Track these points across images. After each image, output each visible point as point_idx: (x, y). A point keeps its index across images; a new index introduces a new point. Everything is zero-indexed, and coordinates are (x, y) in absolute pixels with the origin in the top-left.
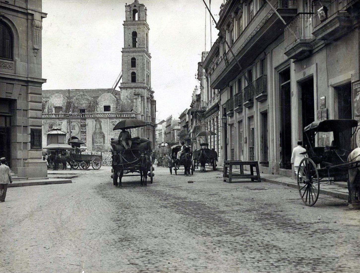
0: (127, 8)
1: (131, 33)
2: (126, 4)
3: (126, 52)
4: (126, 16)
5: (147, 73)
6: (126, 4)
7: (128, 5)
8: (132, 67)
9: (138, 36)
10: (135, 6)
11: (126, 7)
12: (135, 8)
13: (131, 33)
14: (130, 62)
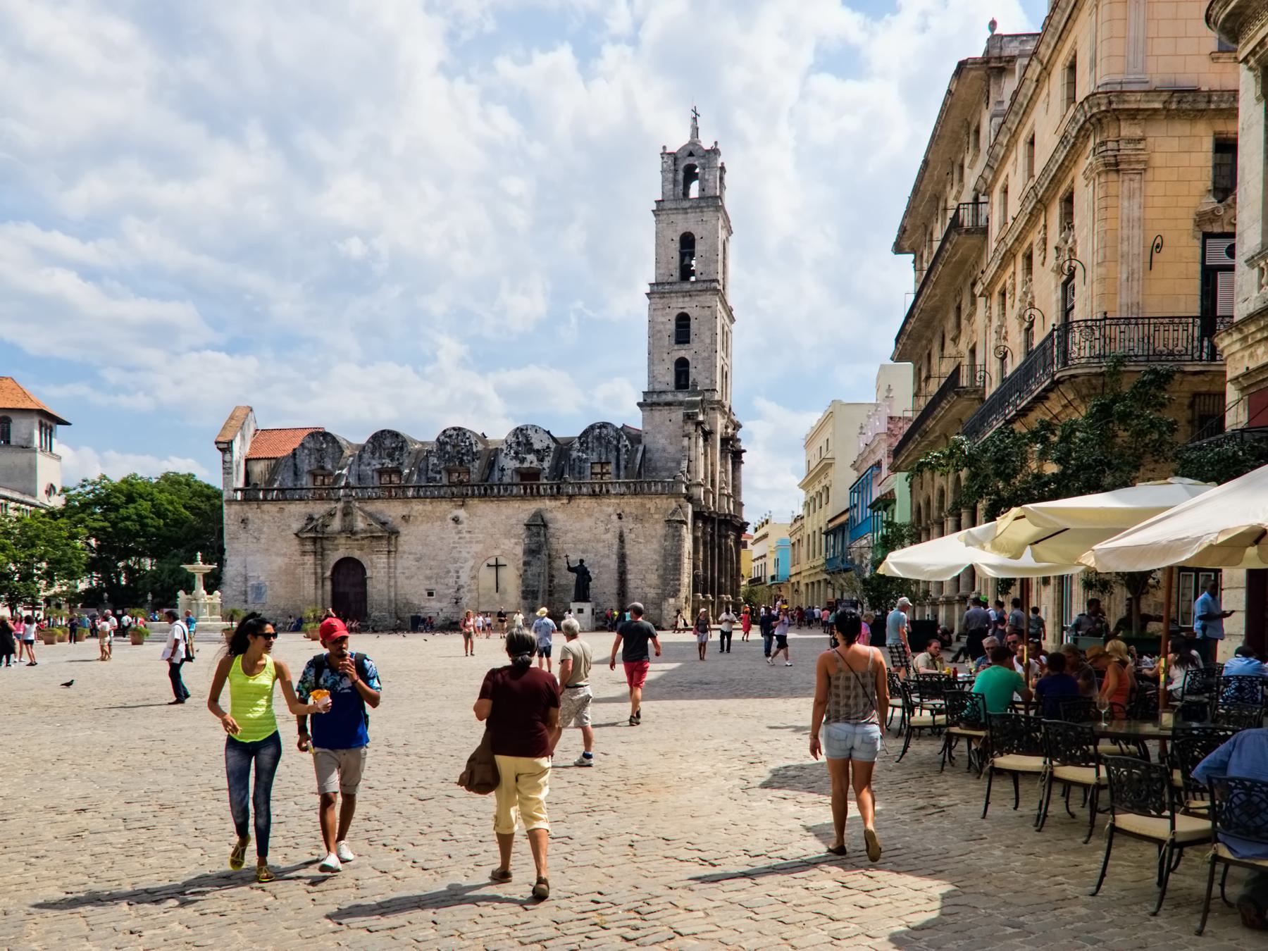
1: (677, 239)
3: (662, 295)
4: (663, 187)
5: (722, 363)
8: (678, 342)
9: (699, 248)
14: (672, 326)
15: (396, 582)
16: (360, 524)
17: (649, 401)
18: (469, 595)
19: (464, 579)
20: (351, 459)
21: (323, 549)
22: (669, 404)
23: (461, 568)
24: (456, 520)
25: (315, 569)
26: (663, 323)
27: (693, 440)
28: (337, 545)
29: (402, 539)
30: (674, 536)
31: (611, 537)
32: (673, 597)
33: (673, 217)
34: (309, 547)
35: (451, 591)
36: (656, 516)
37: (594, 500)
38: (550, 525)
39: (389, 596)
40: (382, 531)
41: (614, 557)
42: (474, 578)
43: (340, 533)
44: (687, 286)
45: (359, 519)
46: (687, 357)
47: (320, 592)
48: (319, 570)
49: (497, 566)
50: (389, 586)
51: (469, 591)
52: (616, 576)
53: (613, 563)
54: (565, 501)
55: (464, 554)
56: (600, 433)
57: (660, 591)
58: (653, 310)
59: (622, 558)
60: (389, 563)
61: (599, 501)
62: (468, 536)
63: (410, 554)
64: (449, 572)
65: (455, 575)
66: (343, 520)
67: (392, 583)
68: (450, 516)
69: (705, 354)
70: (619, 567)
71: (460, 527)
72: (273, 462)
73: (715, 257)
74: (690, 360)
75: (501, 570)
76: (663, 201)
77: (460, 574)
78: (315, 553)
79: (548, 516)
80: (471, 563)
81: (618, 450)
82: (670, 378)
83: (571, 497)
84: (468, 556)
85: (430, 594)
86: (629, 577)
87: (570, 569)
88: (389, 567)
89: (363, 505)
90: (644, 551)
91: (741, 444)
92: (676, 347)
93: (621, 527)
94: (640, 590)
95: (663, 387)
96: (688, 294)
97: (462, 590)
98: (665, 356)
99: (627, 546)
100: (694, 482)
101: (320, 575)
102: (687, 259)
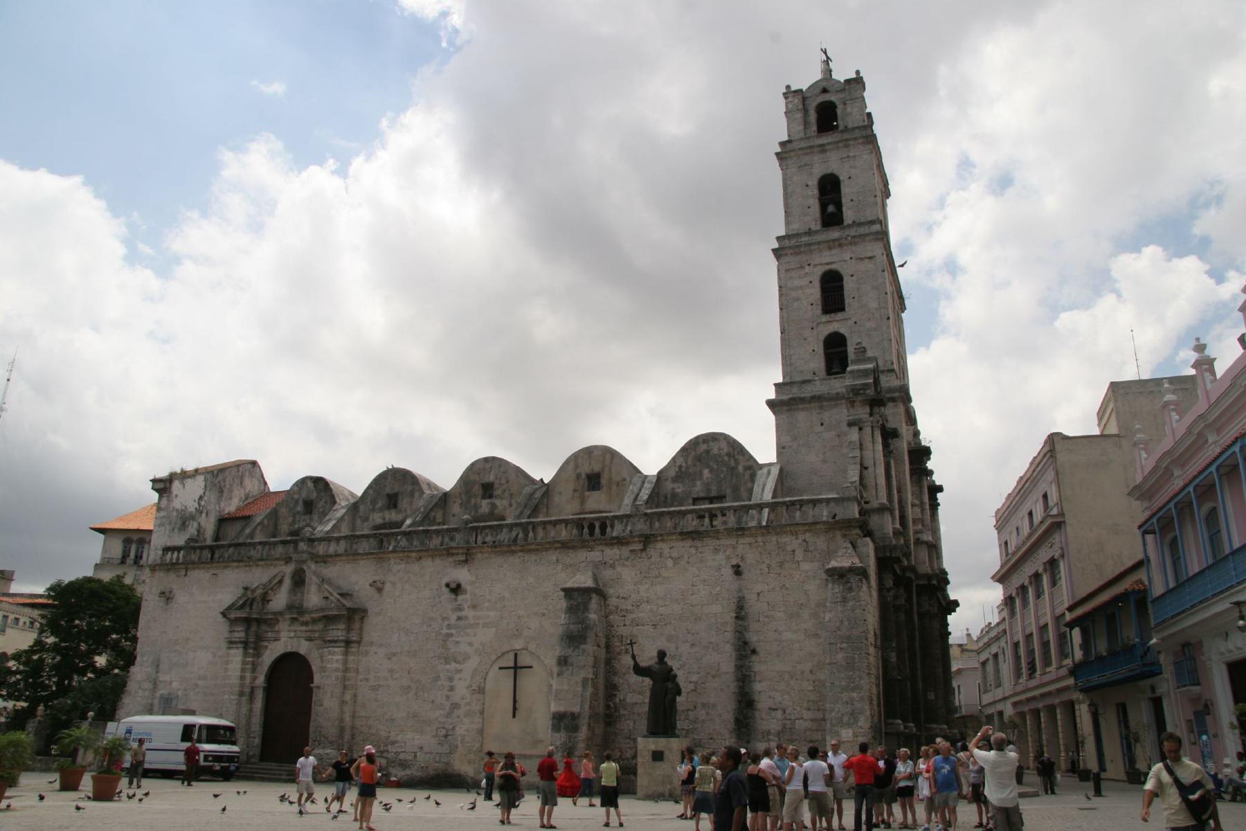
0: (790, 99)
1: (814, 182)
2: (788, 87)
3: (797, 251)
7: (793, 88)
10: (825, 91)
11: (786, 98)
12: (826, 97)
13: (816, 183)
14: (815, 292)
16: (313, 598)
17: (785, 397)
19: (461, 689)
21: (260, 638)
22: (817, 399)
23: (459, 671)
24: (456, 589)
25: (243, 670)
26: (801, 288)
27: (868, 430)
28: (278, 632)
29: (372, 620)
31: (722, 611)
32: (849, 725)
33: (806, 159)
34: (240, 634)
35: (438, 713)
36: (806, 566)
39: (342, 720)
41: (729, 648)
44: (835, 234)
45: (313, 588)
46: (842, 331)
47: (244, 710)
48: (248, 675)
49: (516, 668)
50: (343, 703)
51: (467, 715)
52: (733, 686)
53: (725, 661)
54: (639, 546)
55: (464, 648)
56: (708, 452)
58: (783, 274)
59: (745, 651)
60: (345, 662)
61: (698, 543)
63: (381, 645)
64: (438, 678)
65: (447, 684)
67: (348, 697)
71: (460, 598)
73: (872, 199)
74: (846, 335)
76: (789, 141)
77: (455, 682)
78: (245, 644)
80: (473, 663)
82: (818, 363)
83: (647, 540)
84: (469, 650)
86: (757, 686)
87: (639, 670)
88: (346, 670)
90: (788, 635)
91: (934, 477)
92: (825, 318)
93: (740, 590)
94: (779, 714)
96: (839, 244)
97: (457, 712)
98: (807, 333)
99: (754, 626)
101: (248, 681)
102: (831, 208)
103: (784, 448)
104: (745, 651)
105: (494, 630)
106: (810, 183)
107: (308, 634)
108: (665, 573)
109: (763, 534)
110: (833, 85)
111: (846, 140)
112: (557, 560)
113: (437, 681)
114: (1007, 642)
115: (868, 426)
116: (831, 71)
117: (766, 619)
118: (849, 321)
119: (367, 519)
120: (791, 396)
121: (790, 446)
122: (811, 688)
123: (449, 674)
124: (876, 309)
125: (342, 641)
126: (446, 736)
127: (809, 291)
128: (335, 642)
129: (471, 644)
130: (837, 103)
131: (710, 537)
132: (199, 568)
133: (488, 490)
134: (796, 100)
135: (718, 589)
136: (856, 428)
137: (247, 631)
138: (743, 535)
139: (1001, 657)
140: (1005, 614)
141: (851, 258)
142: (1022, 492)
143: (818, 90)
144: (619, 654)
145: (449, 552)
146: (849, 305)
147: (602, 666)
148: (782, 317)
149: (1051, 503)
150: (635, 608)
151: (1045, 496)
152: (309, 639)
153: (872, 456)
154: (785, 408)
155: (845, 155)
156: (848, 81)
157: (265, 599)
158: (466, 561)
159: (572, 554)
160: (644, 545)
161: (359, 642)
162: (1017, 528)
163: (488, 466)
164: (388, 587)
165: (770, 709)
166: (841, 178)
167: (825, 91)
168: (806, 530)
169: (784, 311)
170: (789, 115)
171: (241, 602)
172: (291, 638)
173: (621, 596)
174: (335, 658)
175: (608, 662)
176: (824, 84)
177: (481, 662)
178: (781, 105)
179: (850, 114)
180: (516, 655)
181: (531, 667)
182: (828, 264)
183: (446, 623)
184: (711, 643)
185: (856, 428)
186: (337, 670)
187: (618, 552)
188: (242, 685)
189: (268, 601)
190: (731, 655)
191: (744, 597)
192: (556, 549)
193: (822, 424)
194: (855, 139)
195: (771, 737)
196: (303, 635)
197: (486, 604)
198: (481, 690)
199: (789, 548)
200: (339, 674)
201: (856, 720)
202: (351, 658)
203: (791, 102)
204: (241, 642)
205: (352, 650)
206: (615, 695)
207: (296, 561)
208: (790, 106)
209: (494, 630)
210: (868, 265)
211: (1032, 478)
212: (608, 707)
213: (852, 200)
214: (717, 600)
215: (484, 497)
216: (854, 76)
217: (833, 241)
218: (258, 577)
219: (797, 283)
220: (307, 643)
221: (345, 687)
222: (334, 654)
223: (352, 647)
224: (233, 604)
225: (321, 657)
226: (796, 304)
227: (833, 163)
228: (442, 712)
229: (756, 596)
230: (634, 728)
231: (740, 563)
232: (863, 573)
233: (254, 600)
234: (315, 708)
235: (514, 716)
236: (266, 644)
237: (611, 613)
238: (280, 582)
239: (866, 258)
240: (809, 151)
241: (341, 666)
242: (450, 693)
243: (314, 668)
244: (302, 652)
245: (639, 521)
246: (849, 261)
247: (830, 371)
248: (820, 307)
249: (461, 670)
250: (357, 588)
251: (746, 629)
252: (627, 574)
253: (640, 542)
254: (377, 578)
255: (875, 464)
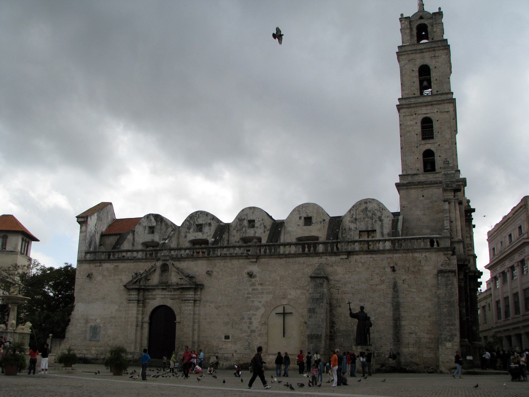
0: (403, 22)
1: (416, 69)
2: (402, 15)
3: (409, 106)
6: (402, 15)
7: (404, 16)
8: (423, 139)
10: (421, 18)
11: (401, 21)
13: (417, 69)
15: (199, 326)
16: (174, 278)
17: (405, 182)
18: (259, 338)
19: (256, 324)
20: (172, 233)
24: (251, 275)
25: (137, 314)
26: (411, 125)
27: (453, 204)
30: (447, 285)
32: (450, 341)
33: (413, 56)
35: (244, 335)
37: (369, 256)
38: (331, 278)
40: (190, 284)
41: (389, 305)
42: (265, 324)
43: (157, 286)
46: (432, 149)
47: (139, 333)
48: (140, 316)
49: (284, 314)
50: (193, 330)
51: (260, 335)
52: (391, 323)
55: (256, 304)
56: (366, 208)
57: (433, 336)
59: (397, 307)
60: (194, 310)
61: (374, 256)
62: (260, 287)
63: (212, 302)
64: (243, 318)
65: (248, 321)
66: (161, 276)
67: (196, 327)
68: (246, 271)
69: (447, 146)
70: (394, 314)
71: (253, 280)
72: (118, 237)
75: (288, 319)
77: (253, 320)
79: (329, 269)
80: (262, 311)
81: (381, 220)
82: (420, 165)
83: (349, 253)
84: (260, 305)
85: (227, 337)
86: (403, 323)
87: (352, 315)
88: (194, 314)
89: (177, 264)
92: (423, 142)
93: (395, 279)
94: (413, 335)
95: (415, 172)
100: (456, 239)
101: (140, 319)
103: (404, 207)
104: (397, 307)
105: (272, 295)
106: (414, 69)
107: (172, 296)
108: (357, 269)
109: (406, 253)
110: (426, 15)
111: (434, 47)
112: (304, 262)
113: (243, 320)
114: (491, 301)
115: (452, 202)
116: (423, 5)
117: (407, 292)
118: (436, 144)
119: (186, 237)
120: (407, 182)
121: (407, 207)
122: (429, 324)
123: (249, 316)
124: (450, 139)
125: (192, 300)
126: (249, 345)
127: (415, 128)
128: (189, 300)
129: (260, 302)
130: (428, 25)
131: (380, 253)
132: (107, 263)
133: (252, 223)
134: (407, 23)
135: (384, 277)
136: (447, 203)
137: (138, 295)
138: (396, 253)
139: (487, 308)
140: (492, 285)
141: (437, 112)
142: (506, 224)
143: (418, 17)
144: (336, 307)
145: (247, 257)
146: (436, 136)
147: (328, 313)
148: (401, 141)
149: (523, 232)
150: (343, 286)
151: (520, 228)
152: (173, 299)
153: (455, 216)
154: (405, 187)
155: (433, 56)
156: (434, 14)
157: (147, 279)
158: (256, 262)
159: (311, 259)
160: (347, 256)
161: (200, 301)
162: (501, 242)
163: (252, 211)
164: (215, 273)
165: (410, 333)
166: (431, 67)
167: (421, 18)
168: (427, 252)
169: (403, 137)
170: (403, 31)
171: (135, 280)
172: (162, 298)
173: (336, 280)
174: (189, 308)
175: (331, 311)
176: (421, 14)
177: (266, 310)
178: (398, 26)
179: (435, 32)
180: (284, 307)
181: (292, 313)
182: (425, 114)
183: (247, 292)
184: (381, 303)
185: (447, 203)
186: (190, 314)
187: (335, 259)
188: (137, 322)
189: (148, 280)
190: (391, 309)
191: (396, 282)
192: (303, 257)
193: (423, 196)
194: (439, 47)
195: (410, 346)
196: (169, 296)
197: (267, 283)
198: (265, 324)
199: (418, 260)
200: (192, 316)
201: (453, 339)
202: (197, 308)
203: (403, 23)
204: (135, 300)
205: (198, 304)
206: (334, 326)
207: (163, 260)
208: (403, 26)
209: (272, 295)
210: (446, 116)
211: (512, 218)
212: (331, 332)
213: (436, 80)
214: (384, 282)
215: (249, 227)
216: (438, 11)
217: (428, 102)
218: (143, 267)
219: (409, 123)
220: (171, 300)
221: (194, 322)
222: (188, 306)
223: (197, 303)
224: (131, 281)
225: (180, 308)
226: (408, 134)
227: (427, 59)
228: (246, 334)
229: (402, 281)
230: (344, 341)
231: (395, 266)
232: (453, 272)
233: (141, 279)
234: (178, 333)
235: (284, 336)
236: (148, 301)
237: (332, 288)
238: (155, 270)
239: (445, 112)
240: (414, 52)
241: (192, 312)
242: (250, 325)
243: (176, 313)
244: (169, 305)
245: (344, 244)
246: (436, 113)
247: (426, 170)
248: (421, 136)
249: (256, 314)
250: (197, 274)
251: (398, 297)
252: (340, 270)
253: (346, 255)
254: (208, 269)
255: (456, 220)
